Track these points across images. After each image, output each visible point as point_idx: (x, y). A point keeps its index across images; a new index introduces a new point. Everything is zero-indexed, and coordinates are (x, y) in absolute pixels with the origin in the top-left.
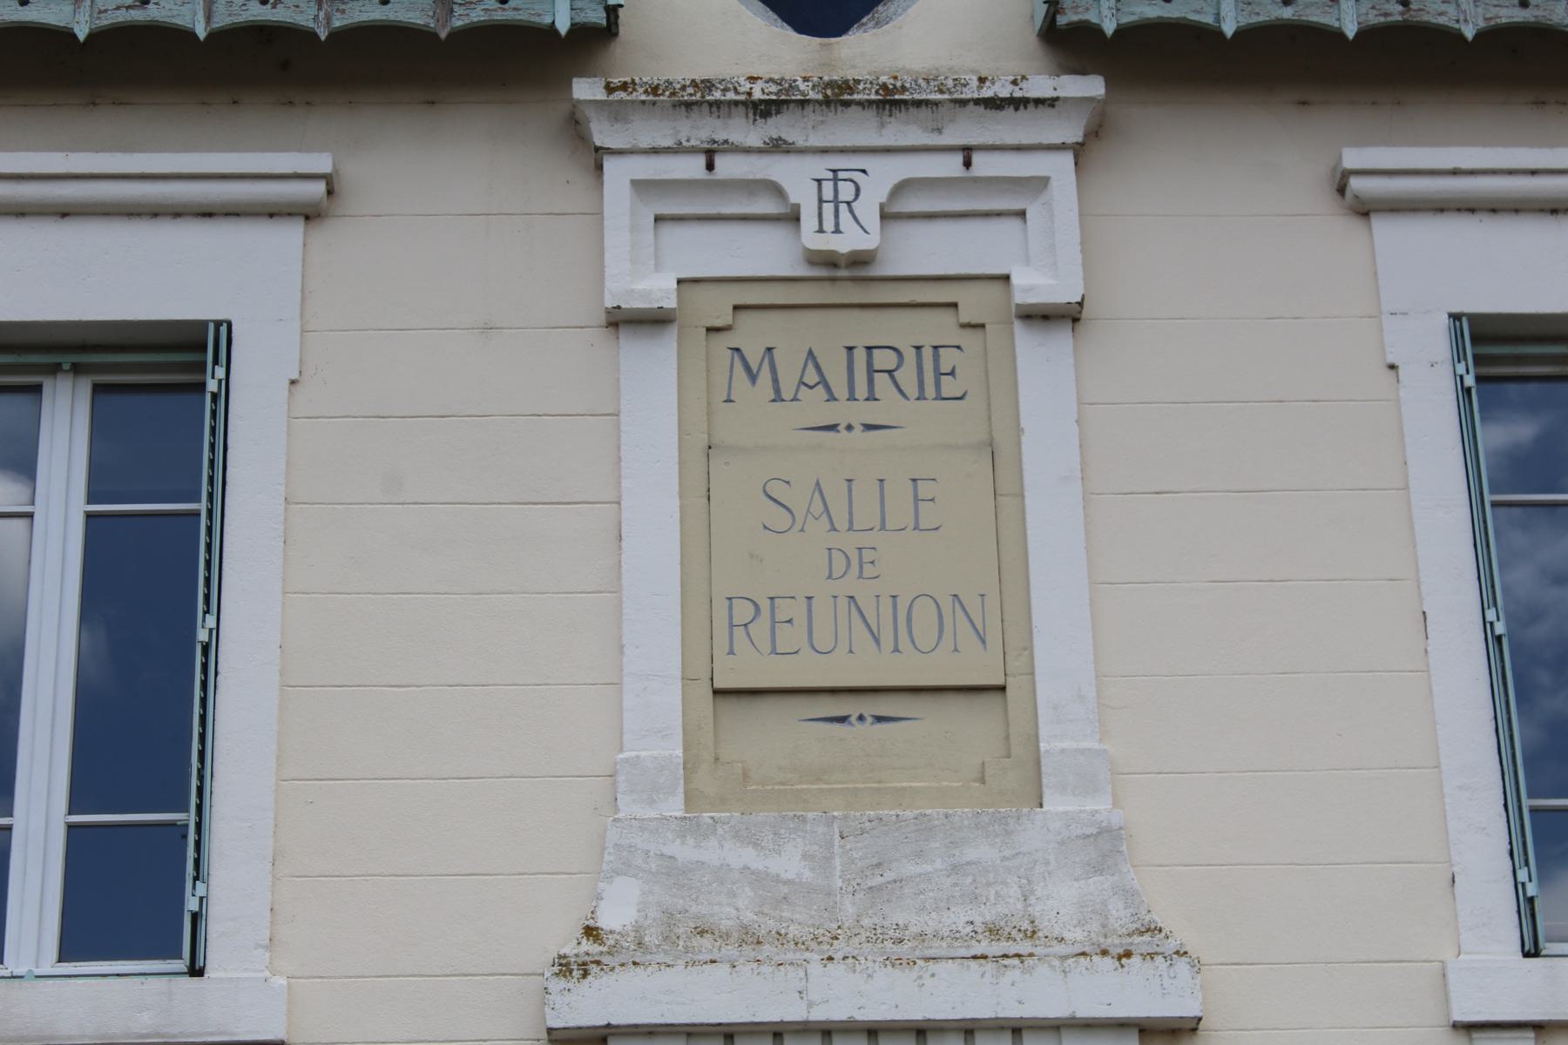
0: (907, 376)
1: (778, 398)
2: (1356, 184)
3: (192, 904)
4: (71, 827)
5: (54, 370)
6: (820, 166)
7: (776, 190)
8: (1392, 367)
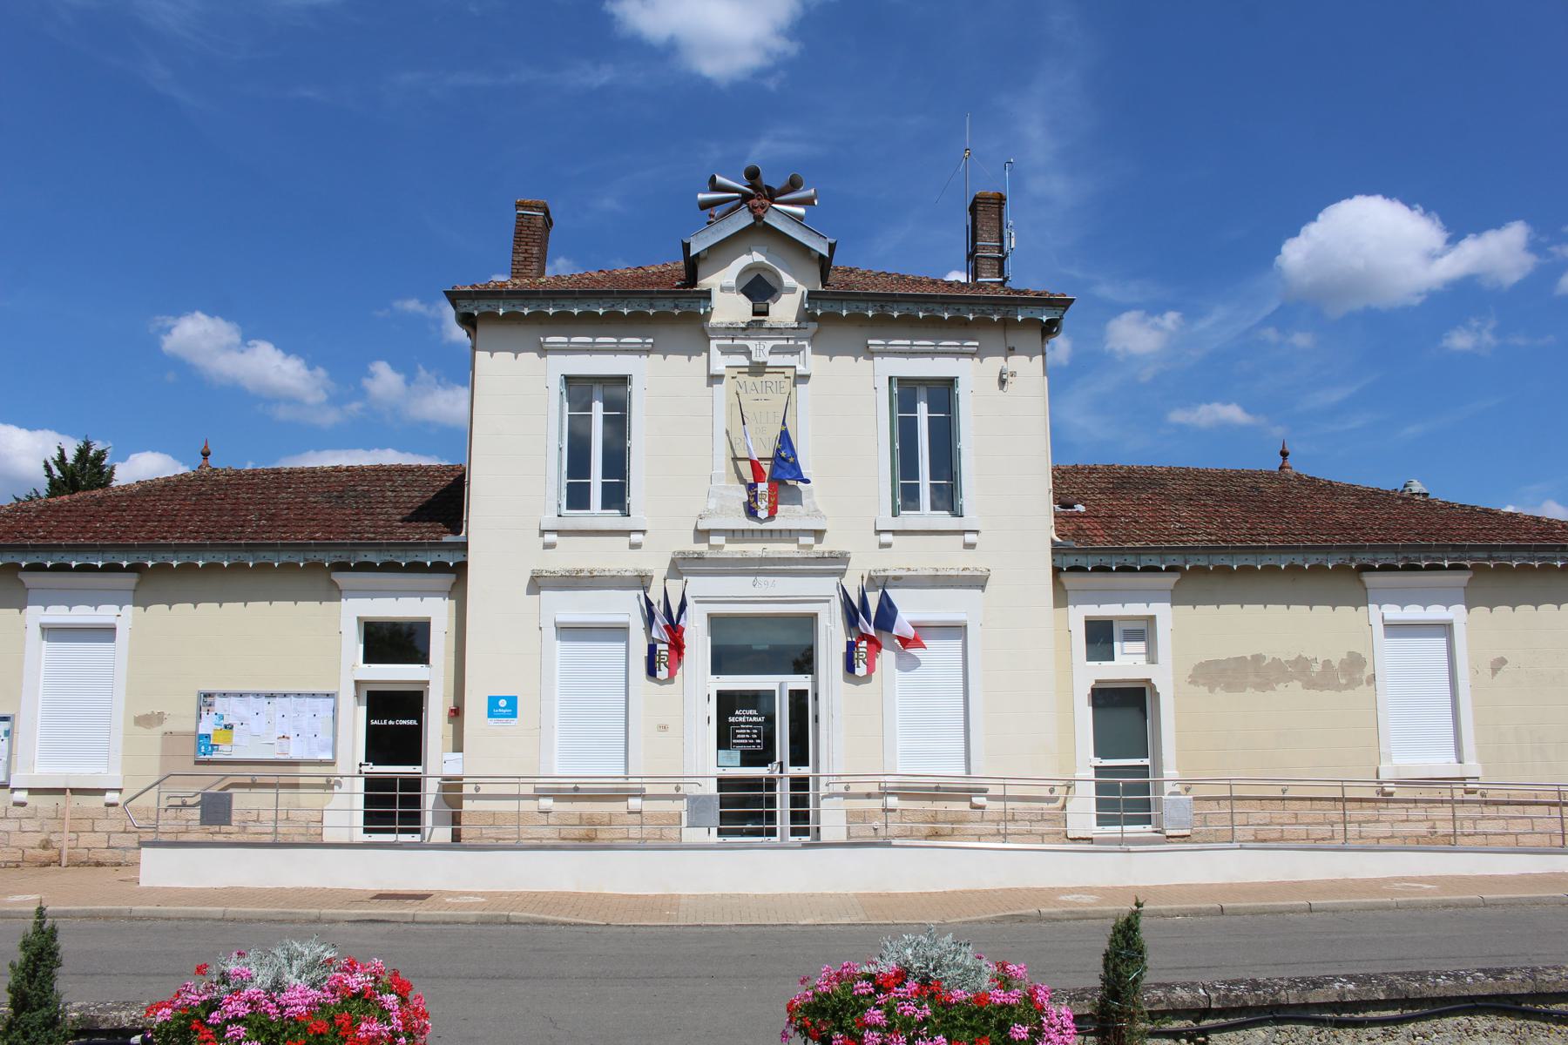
0: (774, 388)
1: (746, 392)
2: (870, 347)
3: (628, 502)
4: (603, 483)
5: (595, 383)
6: (757, 342)
7: (747, 347)
8: (875, 388)
